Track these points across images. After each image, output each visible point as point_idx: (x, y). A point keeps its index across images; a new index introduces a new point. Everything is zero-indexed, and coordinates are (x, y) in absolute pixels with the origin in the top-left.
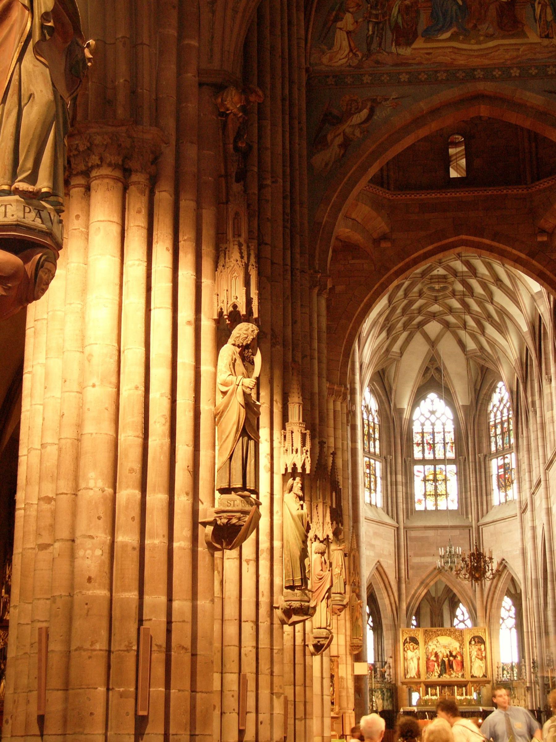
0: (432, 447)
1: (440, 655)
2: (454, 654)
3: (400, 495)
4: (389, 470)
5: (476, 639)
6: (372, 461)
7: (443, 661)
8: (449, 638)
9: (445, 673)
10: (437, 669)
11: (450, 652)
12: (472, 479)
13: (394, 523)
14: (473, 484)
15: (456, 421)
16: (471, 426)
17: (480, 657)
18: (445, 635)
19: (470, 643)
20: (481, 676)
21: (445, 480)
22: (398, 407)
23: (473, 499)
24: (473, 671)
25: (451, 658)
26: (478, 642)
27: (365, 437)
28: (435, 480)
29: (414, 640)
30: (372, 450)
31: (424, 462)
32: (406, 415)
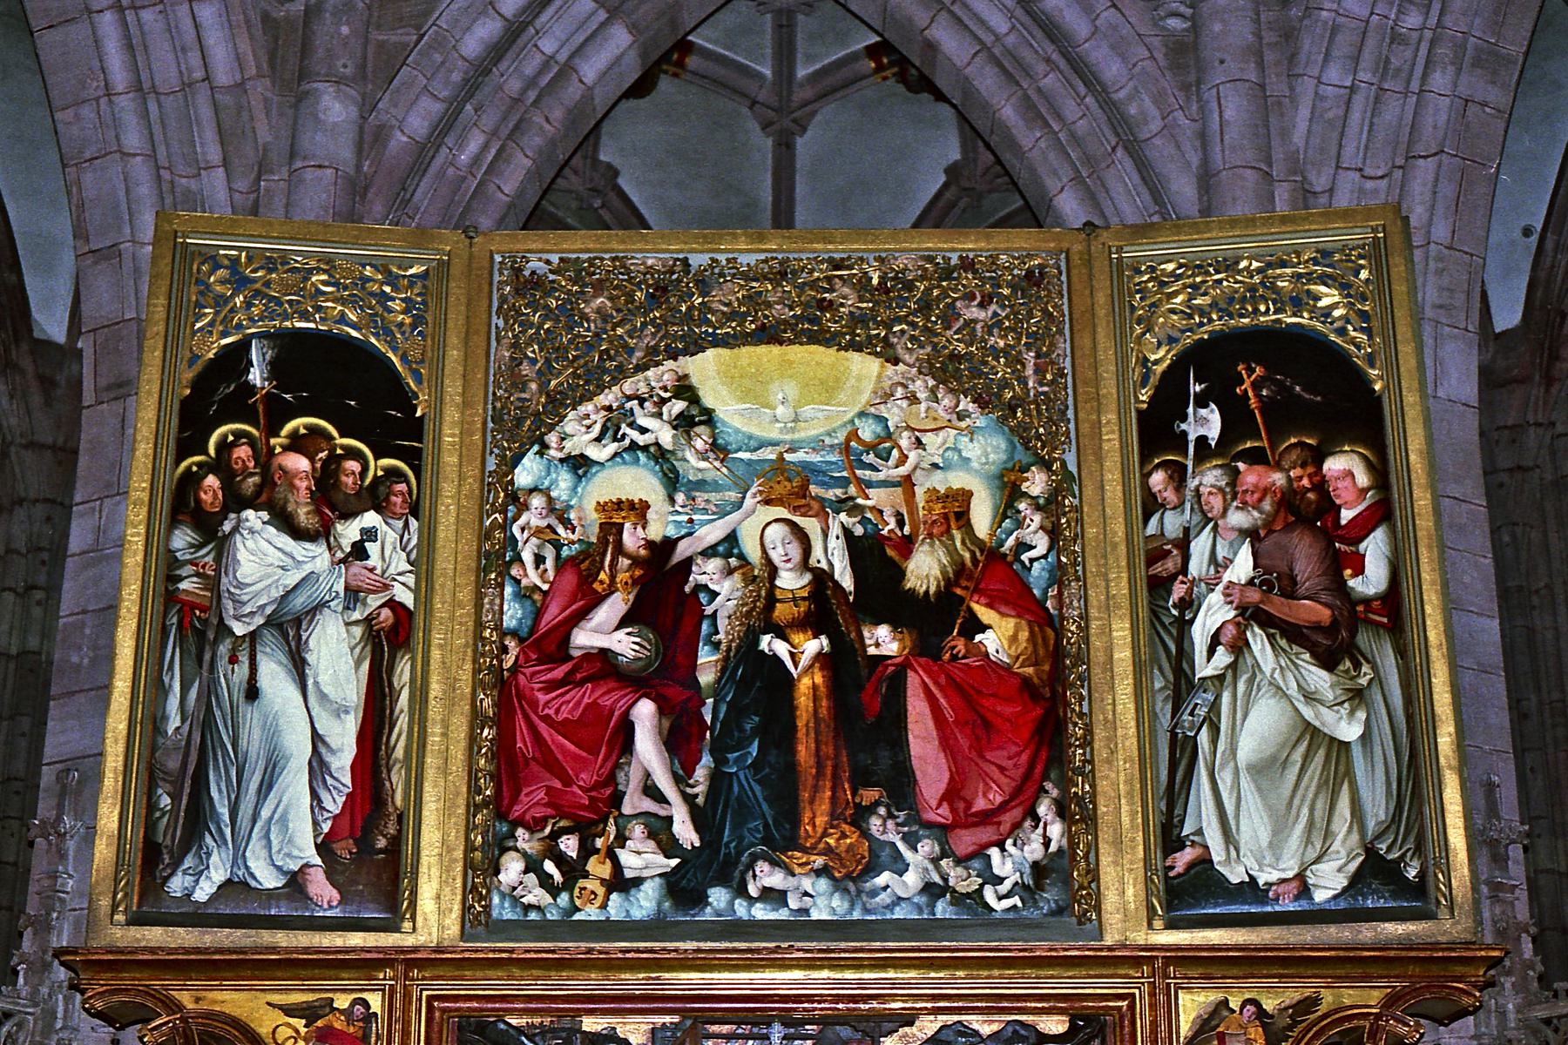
1: (726, 594)
2: (925, 569)
5: (1249, 379)
7: (759, 680)
8: (865, 368)
9: (783, 842)
11: (868, 552)
17: (1312, 611)
19: (1158, 432)
20: (1329, 883)
24: (1202, 816)
25: (883, 640)
26: (1282, 416)
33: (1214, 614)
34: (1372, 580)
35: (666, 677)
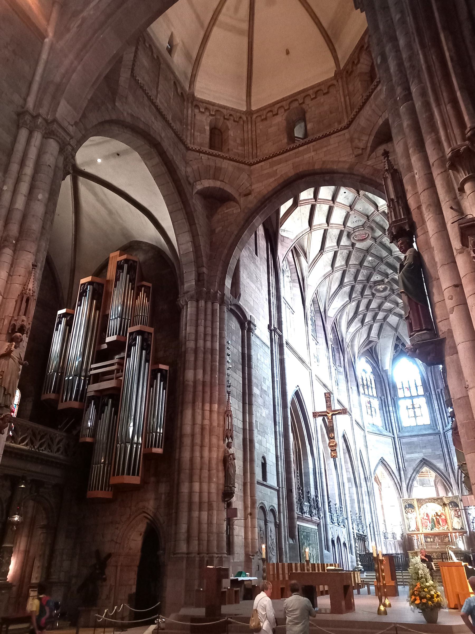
0: (409, 389)
2: (439, 514)
3: (392, 418)
4: (384, 404)
6: (371, 400)
7: (433, 519)
9: (435, 527)
10: (430, 525)
11: (436, 513)
12: (436, 404)
13: (391, 435)
14: (437, 407)
15: (421, 373)
16: (429, 374)
18: (431, 502)
20: (460, 528)
21: (420, 407)
22: (384, 369)
23: (439, 416)
27: (365, 387)
28: (414, 408)
29: (411, 506)
30: (371, 394)
31: (405, 398)
32: (389, 373)
33: (453, 516)
34: (459, 514)
35: (428, 519)
